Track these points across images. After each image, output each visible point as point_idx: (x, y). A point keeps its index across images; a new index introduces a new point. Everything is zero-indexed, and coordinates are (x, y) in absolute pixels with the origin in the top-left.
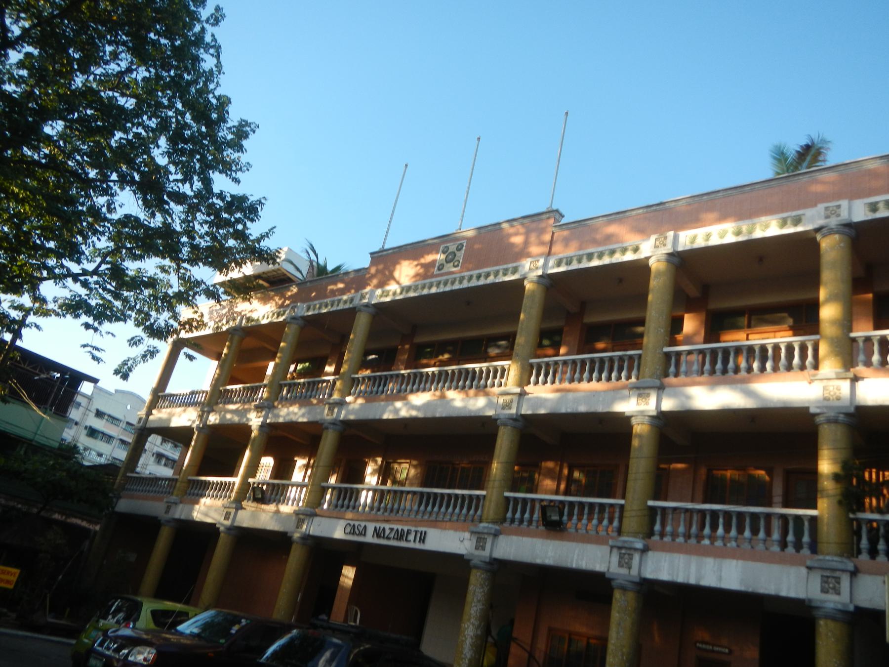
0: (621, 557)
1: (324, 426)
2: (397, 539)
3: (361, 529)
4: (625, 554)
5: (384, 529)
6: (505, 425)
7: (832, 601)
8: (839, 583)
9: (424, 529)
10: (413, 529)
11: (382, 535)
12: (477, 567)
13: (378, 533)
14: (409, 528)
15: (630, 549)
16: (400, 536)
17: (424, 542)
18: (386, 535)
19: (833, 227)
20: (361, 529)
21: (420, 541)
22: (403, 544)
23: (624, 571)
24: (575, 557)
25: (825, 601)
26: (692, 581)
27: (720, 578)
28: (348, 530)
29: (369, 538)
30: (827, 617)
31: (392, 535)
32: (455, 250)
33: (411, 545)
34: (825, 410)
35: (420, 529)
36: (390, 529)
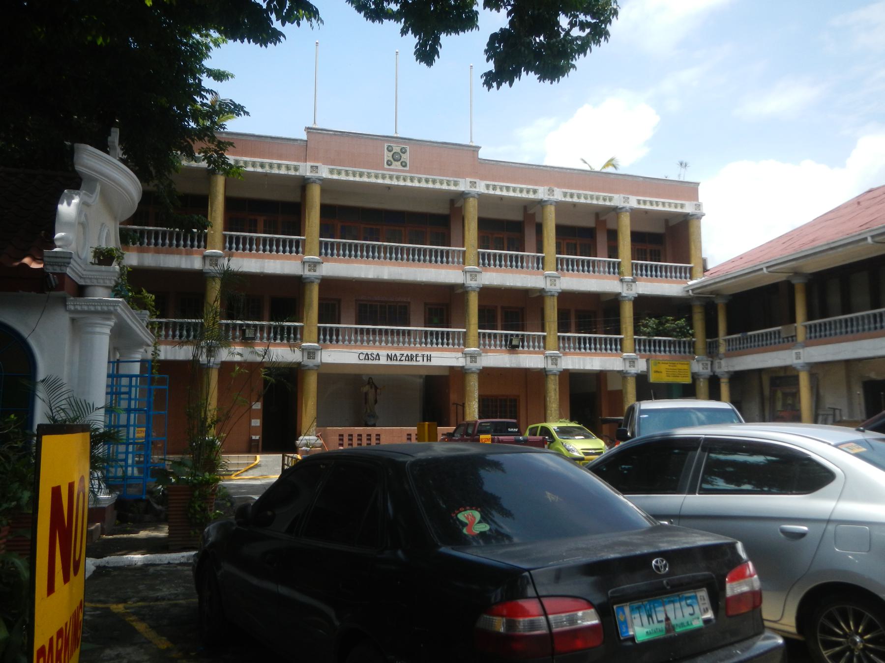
0: (552, 360)
1: (308, 280)
2: (409, 360)
3: (375, 356)
4: (555, 359)
5: (395, 355)
6: (474, 291)
7: (633, 370)
8: (634, 363)
9: (429, 353)
10: (420, 353)
11: (395, 359)
12: (473, 372)
13: (389, 357)
14: (417, 353)
15: (555, 357)
16: (411, 358)
17: (430, 361)
18: (398, 360)
19: (628, 209)
20: (375, 356)
21: (427, 361)
22: (414, 363)
23: (554, 367)
24: (527, 362)
25: (631, 370)
26: (582, 368)
27: (592, 365)
28: (362, 357)
29: (383, 361)
30: (631, 376)
31: (403, 358)
32: (399, 151)
33: (421, 363)
34: (628, 295)
35: (426, 353)
36: (400, 354)
